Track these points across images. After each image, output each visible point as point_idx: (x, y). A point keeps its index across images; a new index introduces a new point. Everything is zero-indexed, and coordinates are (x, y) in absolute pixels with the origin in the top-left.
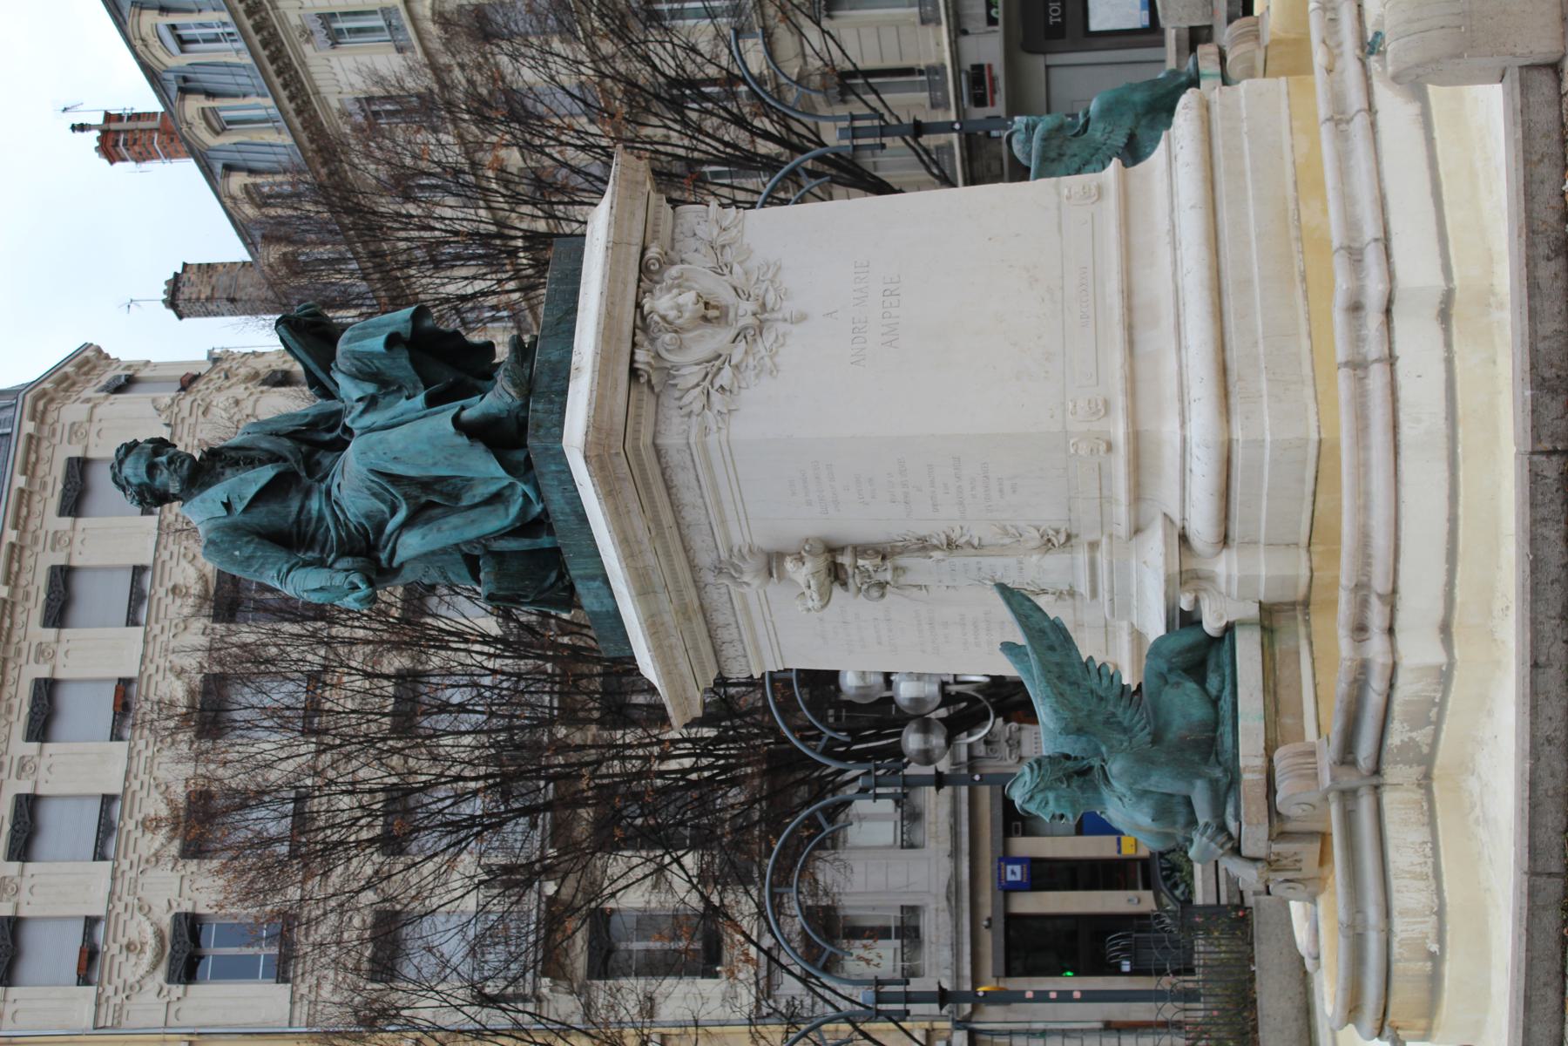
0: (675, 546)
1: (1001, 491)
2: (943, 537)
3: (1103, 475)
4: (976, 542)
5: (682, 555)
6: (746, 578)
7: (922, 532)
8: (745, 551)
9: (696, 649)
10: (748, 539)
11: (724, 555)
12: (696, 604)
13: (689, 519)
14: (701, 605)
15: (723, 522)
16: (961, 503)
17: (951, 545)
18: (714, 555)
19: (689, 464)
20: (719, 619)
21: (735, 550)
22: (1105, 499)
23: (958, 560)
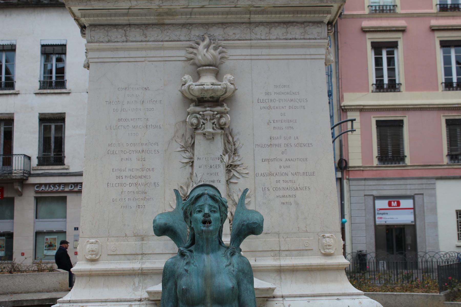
0: (231, 18)
1: (283, 196)
2: (238, 163)
3: (301, 252)
4: (232, 181)
5: (220, 21)
6: (211, 51)
7: (241, 152)
8: (224, 55)
9: (126, 15)
10: (231, 58)
11: (223, 43)
12: (167, 21)
13: (273, 30)
14: (164, 24)
15: (251, 47)
16: (271, 174)
17: (230, 168)
18: (220, 38)
19: (307, 36)
20: (153, 34)
21: (224, 50)
22: (277, 253)
23: (222, 170)
